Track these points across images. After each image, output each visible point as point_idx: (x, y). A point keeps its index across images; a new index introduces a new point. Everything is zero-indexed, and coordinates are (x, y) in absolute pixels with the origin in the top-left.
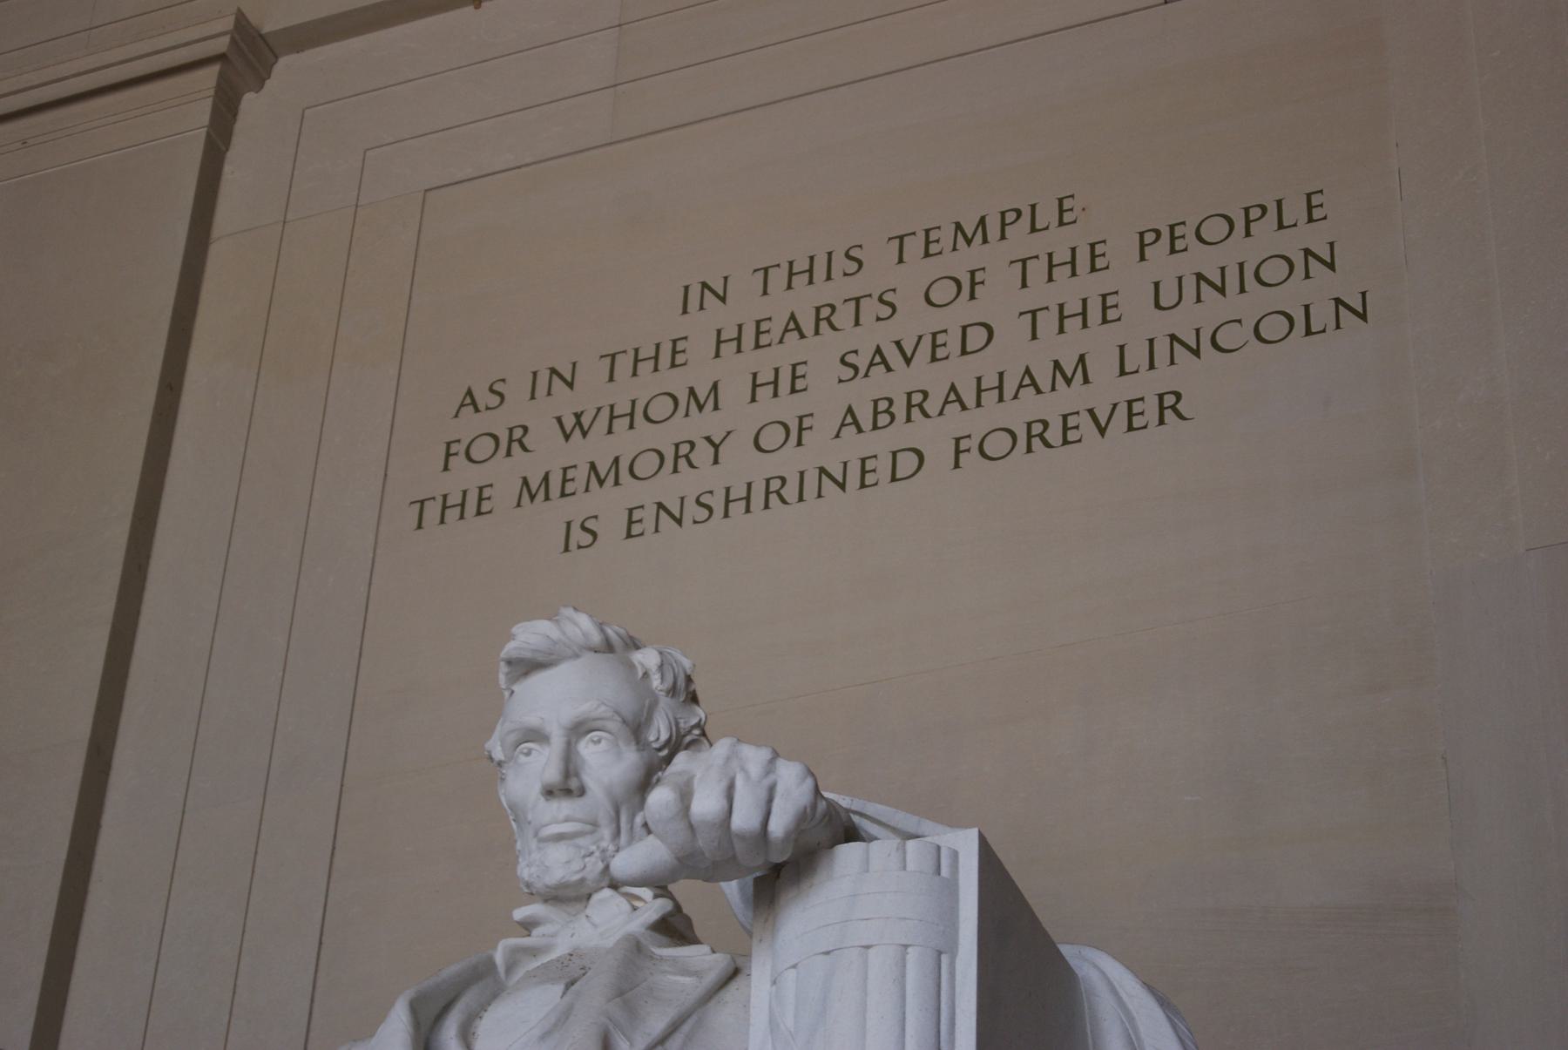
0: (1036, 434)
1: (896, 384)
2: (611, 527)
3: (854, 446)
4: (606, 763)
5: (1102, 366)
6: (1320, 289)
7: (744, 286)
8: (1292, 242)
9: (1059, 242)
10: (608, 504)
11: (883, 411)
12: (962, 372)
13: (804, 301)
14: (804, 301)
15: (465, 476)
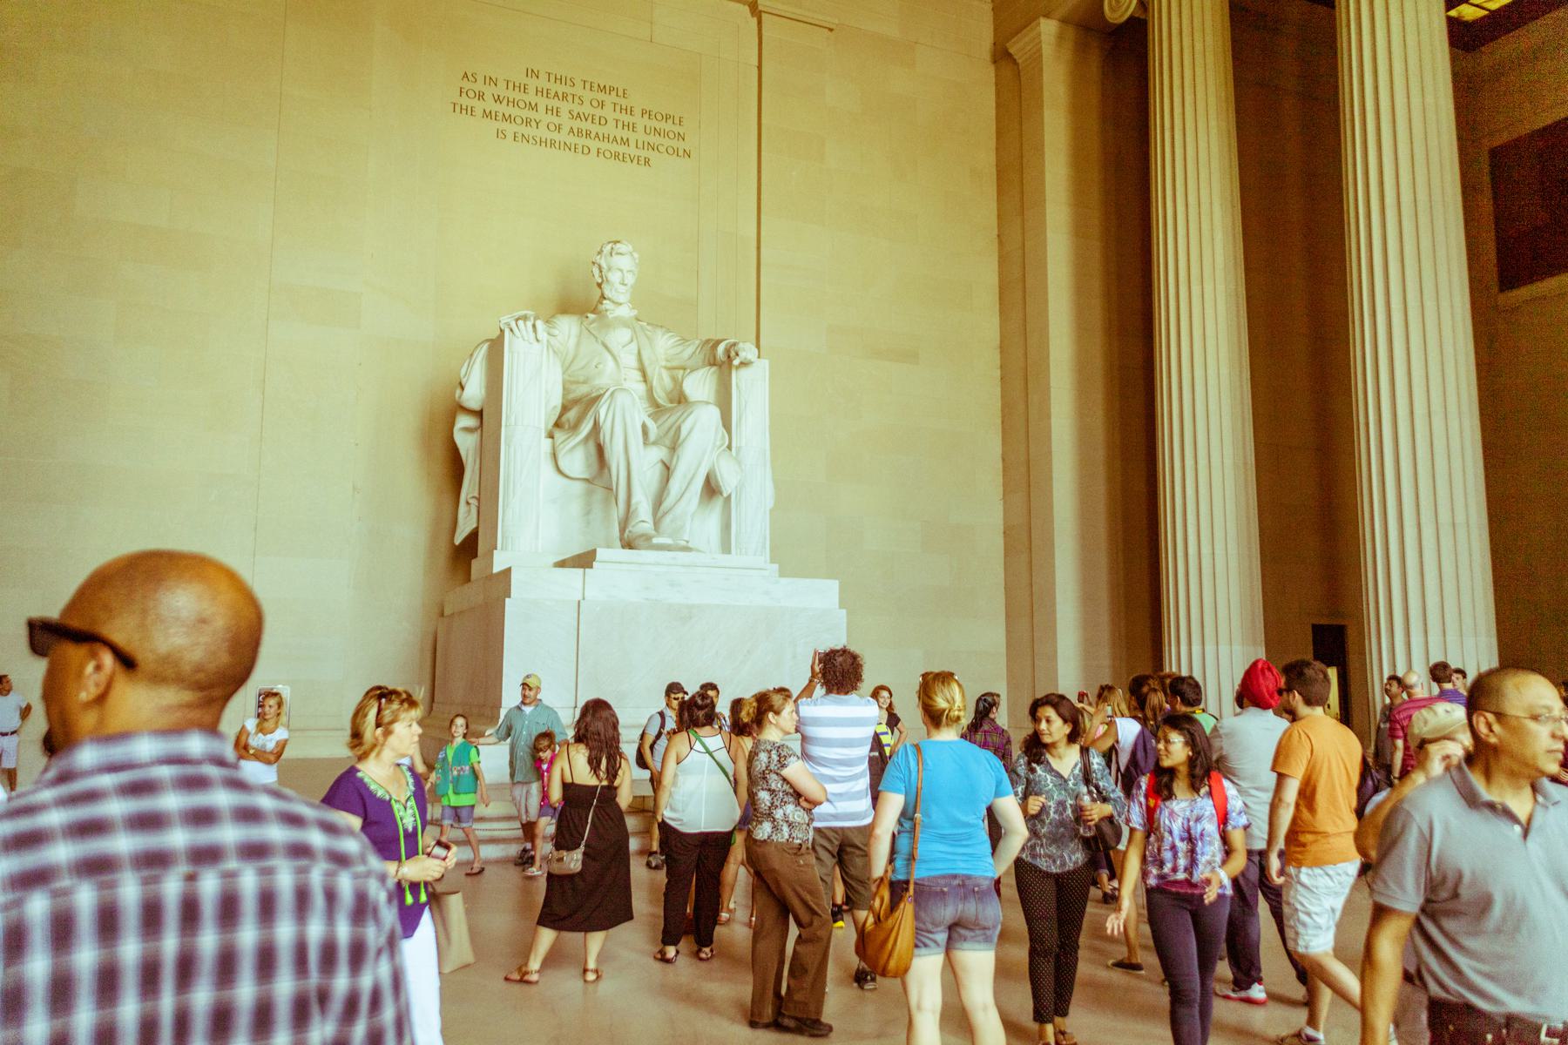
0: (616, 156)
1: (585, 126)
2: (510, 136)
3: (572, 140)
4: (630, 279)
5: (632, 143)
6: (681, 145)
7: (543, 76)
8: (677, 129)
9: (624, 102)
10: (510, 128)
11: (580, 131)
12: (601, 130)
13: (561, 89)
14: (561, 89)
15: (465, 101)
